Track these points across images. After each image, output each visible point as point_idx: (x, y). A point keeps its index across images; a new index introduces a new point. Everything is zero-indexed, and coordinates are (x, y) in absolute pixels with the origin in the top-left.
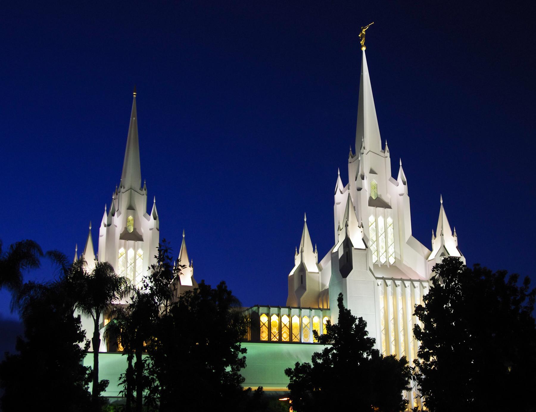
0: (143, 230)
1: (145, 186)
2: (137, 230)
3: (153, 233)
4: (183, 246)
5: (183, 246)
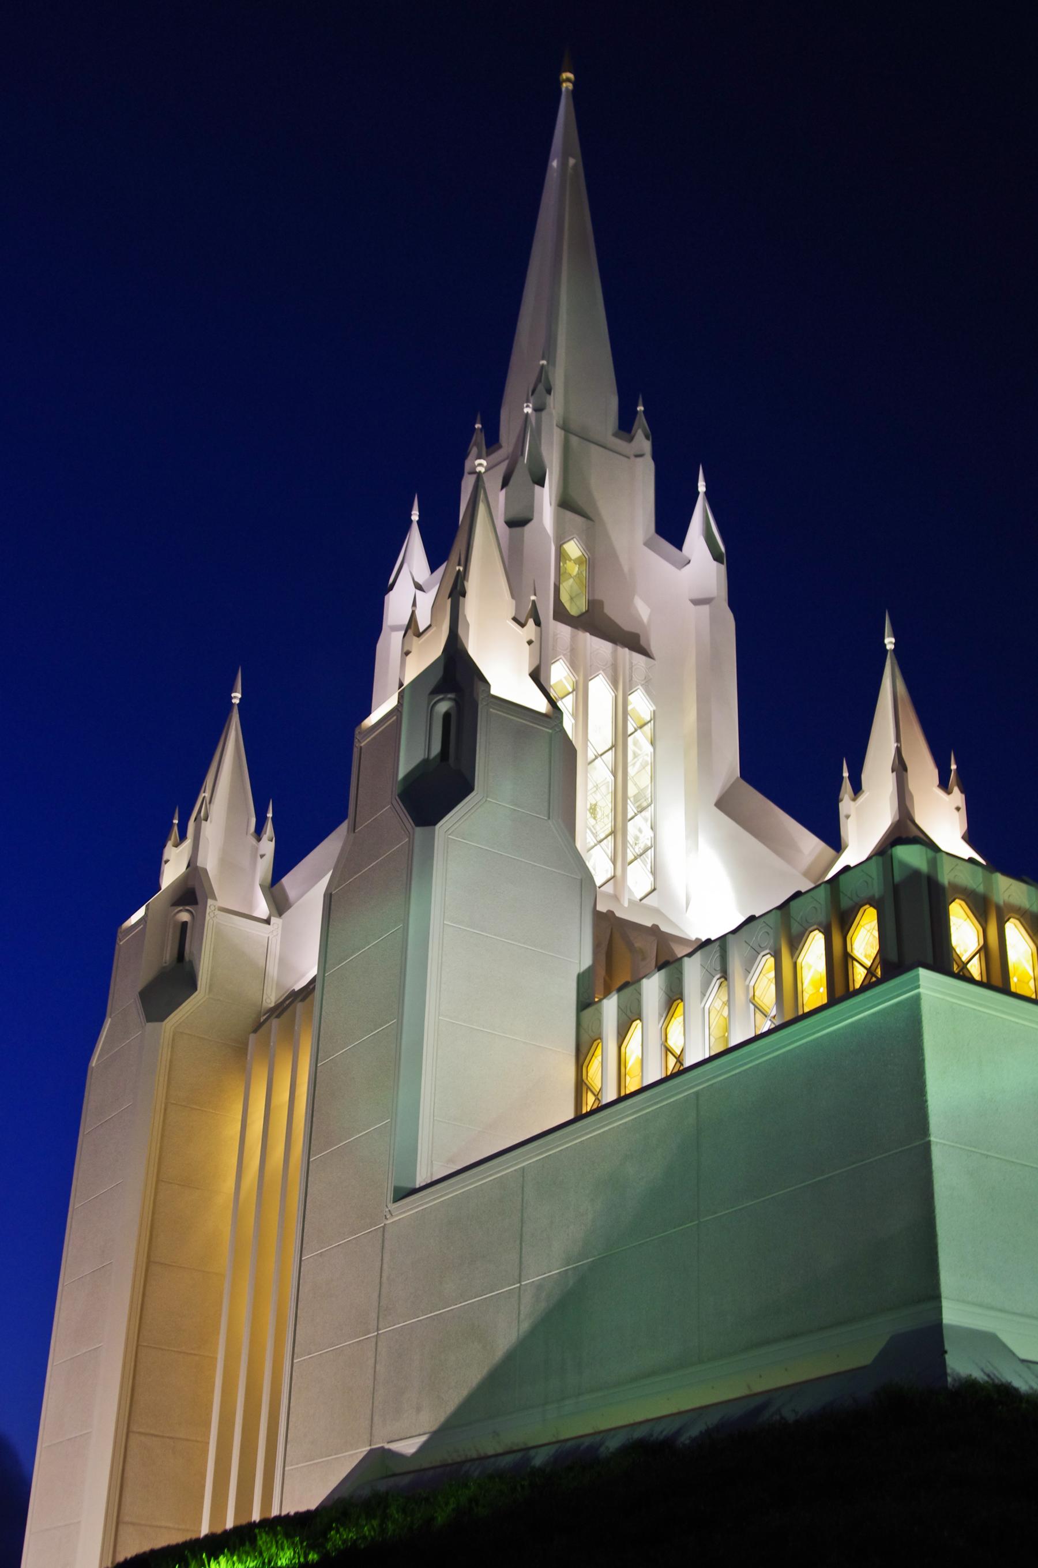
0: (643, 610)
1: (641, 421)
2: (612, 611)
3: (713, 619)
4: (890, 688)
5: (890, 688)
